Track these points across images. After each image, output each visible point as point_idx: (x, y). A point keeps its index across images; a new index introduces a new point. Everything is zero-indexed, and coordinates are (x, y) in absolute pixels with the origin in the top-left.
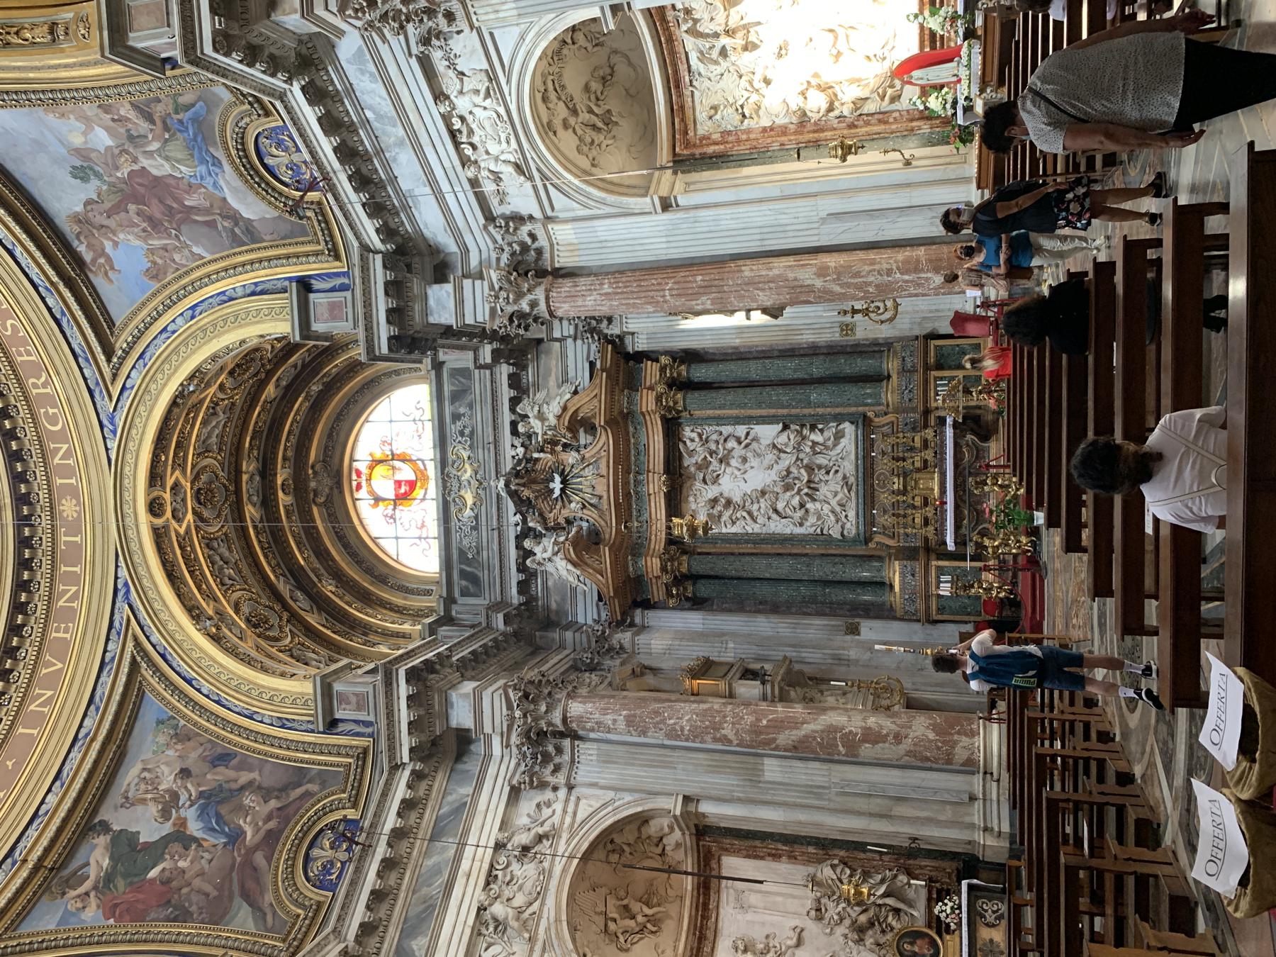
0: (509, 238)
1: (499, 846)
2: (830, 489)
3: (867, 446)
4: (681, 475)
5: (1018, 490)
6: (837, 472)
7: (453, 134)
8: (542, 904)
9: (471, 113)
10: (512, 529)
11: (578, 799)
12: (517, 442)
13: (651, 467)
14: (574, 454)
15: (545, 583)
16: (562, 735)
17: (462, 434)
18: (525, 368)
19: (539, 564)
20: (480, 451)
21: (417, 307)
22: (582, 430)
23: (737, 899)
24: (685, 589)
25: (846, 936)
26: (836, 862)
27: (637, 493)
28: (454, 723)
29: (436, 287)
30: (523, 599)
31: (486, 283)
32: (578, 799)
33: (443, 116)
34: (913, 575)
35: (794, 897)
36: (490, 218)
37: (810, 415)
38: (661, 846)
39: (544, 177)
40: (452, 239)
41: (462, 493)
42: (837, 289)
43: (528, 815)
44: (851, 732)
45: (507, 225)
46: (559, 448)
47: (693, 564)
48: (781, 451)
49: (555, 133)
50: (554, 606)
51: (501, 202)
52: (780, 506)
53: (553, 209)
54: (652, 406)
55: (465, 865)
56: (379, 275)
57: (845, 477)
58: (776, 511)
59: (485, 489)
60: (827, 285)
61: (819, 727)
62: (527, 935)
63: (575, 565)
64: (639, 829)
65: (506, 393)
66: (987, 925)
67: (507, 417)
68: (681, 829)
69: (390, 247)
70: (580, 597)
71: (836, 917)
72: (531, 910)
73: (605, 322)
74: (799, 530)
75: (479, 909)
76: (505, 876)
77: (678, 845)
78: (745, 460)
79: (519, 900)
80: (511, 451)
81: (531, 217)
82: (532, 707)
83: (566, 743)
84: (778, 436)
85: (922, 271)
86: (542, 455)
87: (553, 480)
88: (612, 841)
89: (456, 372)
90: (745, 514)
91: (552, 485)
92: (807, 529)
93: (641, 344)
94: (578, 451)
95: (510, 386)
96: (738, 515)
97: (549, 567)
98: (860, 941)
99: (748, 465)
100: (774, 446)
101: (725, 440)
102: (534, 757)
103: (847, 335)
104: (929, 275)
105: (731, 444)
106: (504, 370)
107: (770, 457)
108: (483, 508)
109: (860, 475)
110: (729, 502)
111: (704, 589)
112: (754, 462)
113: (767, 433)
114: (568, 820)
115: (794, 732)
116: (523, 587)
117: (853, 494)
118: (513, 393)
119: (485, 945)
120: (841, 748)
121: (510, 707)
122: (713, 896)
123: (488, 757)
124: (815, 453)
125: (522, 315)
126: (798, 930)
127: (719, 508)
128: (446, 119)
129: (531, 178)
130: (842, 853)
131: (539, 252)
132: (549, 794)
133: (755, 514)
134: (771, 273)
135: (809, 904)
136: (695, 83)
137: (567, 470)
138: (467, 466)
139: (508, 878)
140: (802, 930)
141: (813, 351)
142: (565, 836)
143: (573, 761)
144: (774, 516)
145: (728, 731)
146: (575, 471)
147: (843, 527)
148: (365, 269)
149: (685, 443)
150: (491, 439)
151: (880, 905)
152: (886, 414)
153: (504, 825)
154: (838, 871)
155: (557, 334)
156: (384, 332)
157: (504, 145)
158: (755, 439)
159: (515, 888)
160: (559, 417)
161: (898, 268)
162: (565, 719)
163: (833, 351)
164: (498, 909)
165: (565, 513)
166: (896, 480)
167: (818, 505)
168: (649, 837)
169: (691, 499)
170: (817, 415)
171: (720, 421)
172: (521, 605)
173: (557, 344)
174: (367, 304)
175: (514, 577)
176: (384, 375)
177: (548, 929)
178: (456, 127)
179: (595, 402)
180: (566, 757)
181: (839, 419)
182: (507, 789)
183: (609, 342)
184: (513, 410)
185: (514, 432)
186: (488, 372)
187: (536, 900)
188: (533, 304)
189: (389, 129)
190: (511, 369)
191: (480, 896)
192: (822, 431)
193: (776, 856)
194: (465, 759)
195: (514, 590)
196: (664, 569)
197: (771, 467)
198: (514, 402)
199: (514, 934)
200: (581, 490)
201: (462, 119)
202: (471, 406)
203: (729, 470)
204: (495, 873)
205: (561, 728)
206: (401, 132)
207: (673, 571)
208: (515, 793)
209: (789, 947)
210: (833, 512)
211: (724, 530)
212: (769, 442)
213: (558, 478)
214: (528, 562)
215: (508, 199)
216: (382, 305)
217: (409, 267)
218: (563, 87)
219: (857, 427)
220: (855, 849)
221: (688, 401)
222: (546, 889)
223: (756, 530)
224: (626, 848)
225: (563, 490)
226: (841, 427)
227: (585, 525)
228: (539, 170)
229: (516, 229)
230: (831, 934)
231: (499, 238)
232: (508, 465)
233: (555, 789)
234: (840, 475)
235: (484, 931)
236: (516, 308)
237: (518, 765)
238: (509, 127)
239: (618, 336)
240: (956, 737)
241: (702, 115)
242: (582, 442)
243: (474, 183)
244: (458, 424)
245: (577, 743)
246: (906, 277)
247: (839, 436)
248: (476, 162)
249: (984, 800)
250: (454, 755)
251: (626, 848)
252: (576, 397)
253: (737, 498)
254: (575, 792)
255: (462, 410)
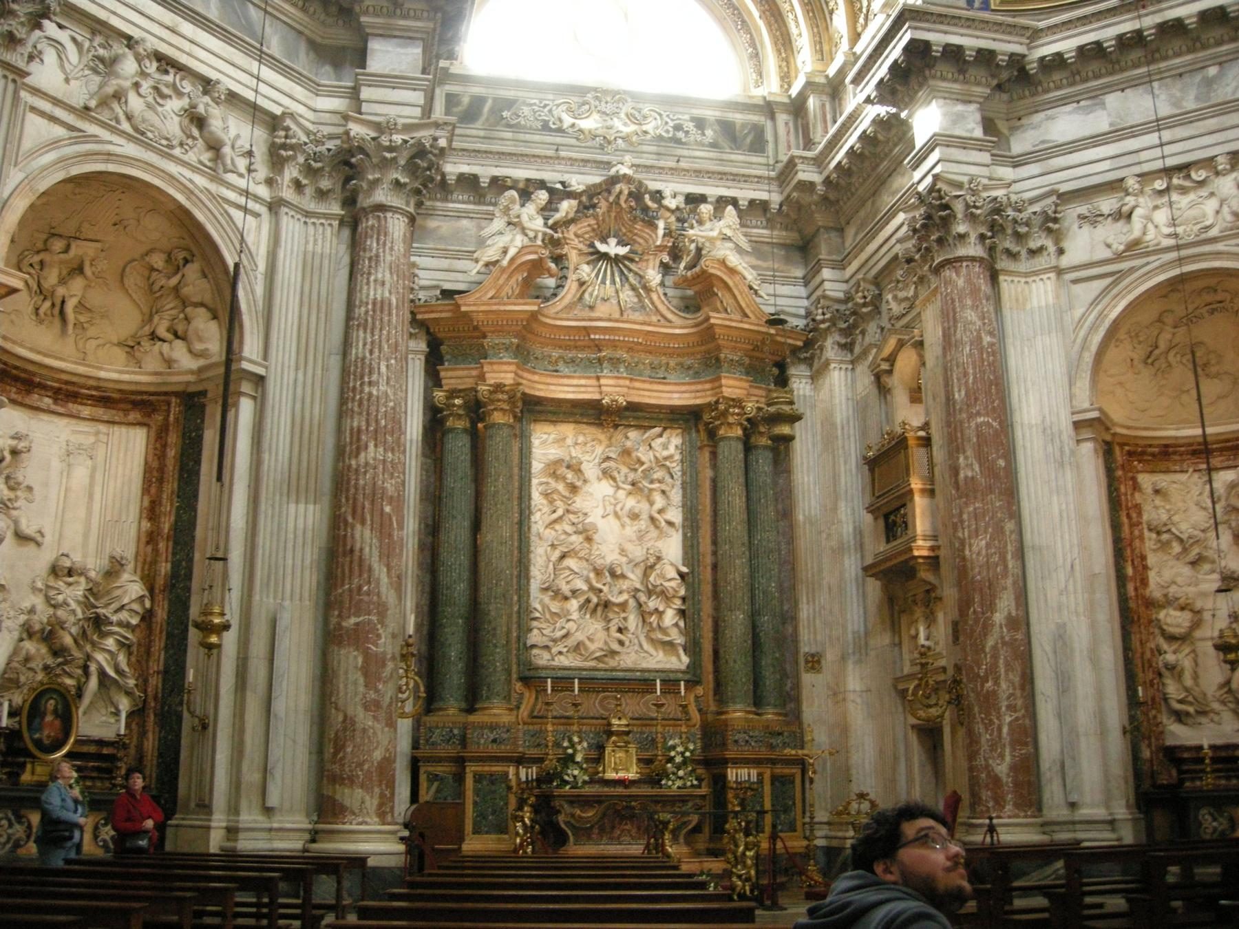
0: (1037, 221)
1: (207, 84)
2: (593, 633)
3: (670, 684)
4: (616, 426)
5: (739, 877)
6: (621, 643)
7: (1184, 168)
8: (129, 137)
9: (1212, 194)
10: (558, 177)
11: (257, 215)
12: (680, 200)
13: (637, 385)
14: (658, 278)
15: (467, 215)
16: (350, 201)
17: (678, 128)
18: (770, 224)
19: (507, 210)
20: (654, 149)
21: (956, 87)
22: (690, 292)
23: (79, 447)
24: (460, 416)
25: (32, 611)
26: (148, 604)
27: (600, 361)
28: (375, 45)
29: (978, 117)
30: (451, 179)
31: (985, 181)
32: (257, 215)
33: (1212, 158)
34: (494, 741)
35: (86, 536)
36: (1066, 197)
37: (699, 611)
38: (169, 336)
39: (1120, 276)
40: (1029, 148)
41: (596, 116)
42: (990, 643)
43: (238, 136)
44: (379, 636)
45: (1056, 220)
46: (666, 259)
47: (505, 432)
48: (649, 568)
49: (1165, 296)
50: (432, 224)
51: (1081, 217)
52: (570, 562)
53: (1075, 282)
54: (727, 392)
55: (187, 28)
56: (1006, 46)
57: (613, 653)
58: (563, 557)
59: (602, 147)
60: (997, 629)
61: (383, 589)
62: (93, 104)
63: (513, 260)
64: (202, 305)
65: (746, 194)
66: (96, 828)
67: (713, 191)
68: (201, 370)
69: (1032, 68)
70: (445, 263)
71: (60, 598)
72: (122, 117)
73: (843, 341)
74: (534, 586)
75: (129, 38)
76: (167, 86)
77: (169, 362)
78: (634, 516)
79: (135, 103)
80: (673, 191)
81: (1061, 252)
82: (402, 162)
83: (336, 209)
84: (672, 564)
85: (1013, 750)
86: (661, 232)
87: (618, 244)
88: (186, 261)
89: (758, 132)
90: (560, 512)
91: (613, 241)
92: (538, 600)
93: (800, 385)
94: (662, 284)
95: (752, 202)
96: (559, 503)
97: (498, 224)
98: (28, 632)
99: (627, 521)
100: (659, 558)
101: (663, 492)
102: (317, 157)
103: (807, 662)
104: (1008, 758)
105: (659, 501)
106: (775, 198)
107: (638, 553)
108: (573, 142)
109: (620, 674)
110: (574, 489)
111: (458, 448)
112: (631, 530)
113: (672, 548)
114: (232, 195)
115: (376, 553)
116: (469, 182)
117: (592, 664)
118: (743, 203)
119: (79, 38)
120: (353, 620)
121: (408, 128)
122: (86, 411)
123: (316, 89)
124: (643, 614)
125: (946, 222)
126: (39, 539)
127: (570, 476)
128: (1209, 162)
129: (1119, 257)
130: (161, 614)
131: (1013, 256)
132: (262, 172)
133: (557, 527)
134: (1009, 556)
135: (77, 557)
136: (1196, 475)
137: (633, 266)
138: (633, 128)
139: (166, 91)
140: (38, 544)
141: (789, 618)
142: (213, 187)
143: (308, 214)
144: (557, 554)
145: (372, 453)
146: (631, 276)
147: (547, 647)
148: (1012, 29)
149: (660, 435)
150: (683, 164)
151: (86, 668)
152: (700, 710)
153: (232, 97)
154: (136, 607)
155: (826, 273)
156: (938, 38)
157: (1167, 230)
158: (662, 535)
159: (150, 99)
160: (723, 262)
161: (1017, 719)
162: (381, 208)
163: (787, 641)
164: (129, 66)
165: (573, 256)
166: (624, 722)
167: (575, 616)
168: (187, 319)
169: (581, 439)
170: (700, 620)
171: (690, 488)
172: (443, 175)
173: (799, 272)
174: (970, 23)
175: (485, 171)
176: (752, 38)
177: (95, 139)
178: (1194, 175)
179: (738, 317)
180: (312, 206)
181: (693, 647)
182: (278, 111)
183: (809, 344)
184: (721, 202)
185: (694, 200)
186: (773, 174)
187: (136, 129)
188: (962, 237)
189: (1192, 94)
190: (774, 206)
191: (152, 44)
192: (676, 625)
193: (152, 512)
194: (312, 55)
195: (465, 169)
196: (498, 388)
197: (623, 552)
198: (734, 202)
199: (94, 87)
200: (603, 282)
201: (1202, 184)
202: (714, 145)
203: (621, 494)
204: (172, 71)
205: (364, 202)
206: (1190, 104)
207: (492, 401)
208: (273, 123)
209: (16, 522)
210: (566, 636)
211: (535, 482)
212: (664, 555)
213: (622, 251)
214: (514, 193)
215: (1087, 228)
216: (969, 41)
217: (999, 87)
218: (1212, 312)
219: (683, 672)
220: (170, 636)
221: (733, 443)
222: (148, 146)
223: (534, 529)
224: (174, 281)
225: (605, 256)
226: (681, 652)
227: (551, 282)
228: (1132, 270)
229: (1049, 231)
230: (35, 589)
231: (1037, 208)
232: (653, 186)
233: (270, 182)
234: (615, 647)
235: (99, 40)
236: (960, 216)
237: (308, 133)
238: (1191, 238)
239: (812, 358)
240: (377, 790)
241: (1162, 480)
242: (668, 291)
243: (1115, 186)
244: (691, 125)
245: (336, 223)
246: (1005, 730)
247: (669, 646)
248: (1142, 192)
249: (270, 830)
250: (319, 40)
251: (174, 281)
252: (747, 289)
253: (579, 502)
254: (263, 210)
255: (709, 133)
